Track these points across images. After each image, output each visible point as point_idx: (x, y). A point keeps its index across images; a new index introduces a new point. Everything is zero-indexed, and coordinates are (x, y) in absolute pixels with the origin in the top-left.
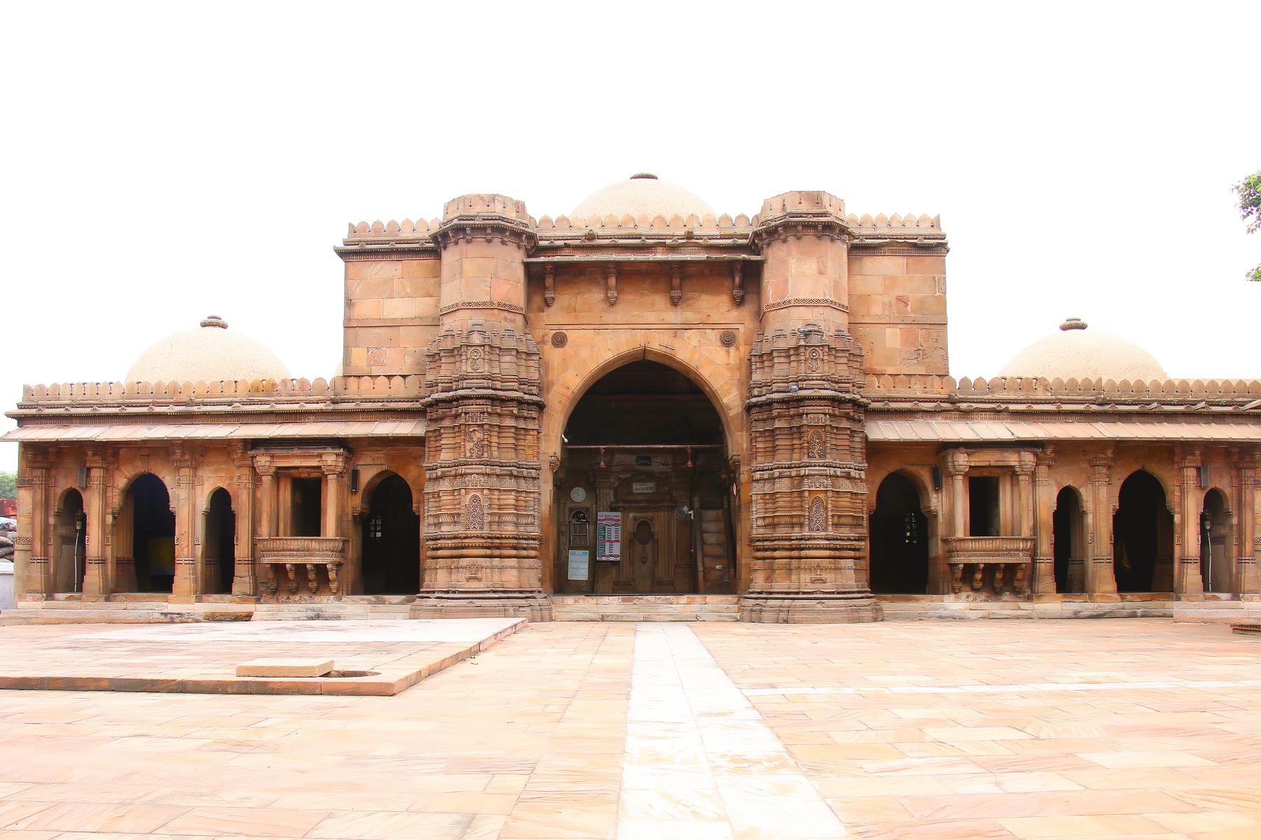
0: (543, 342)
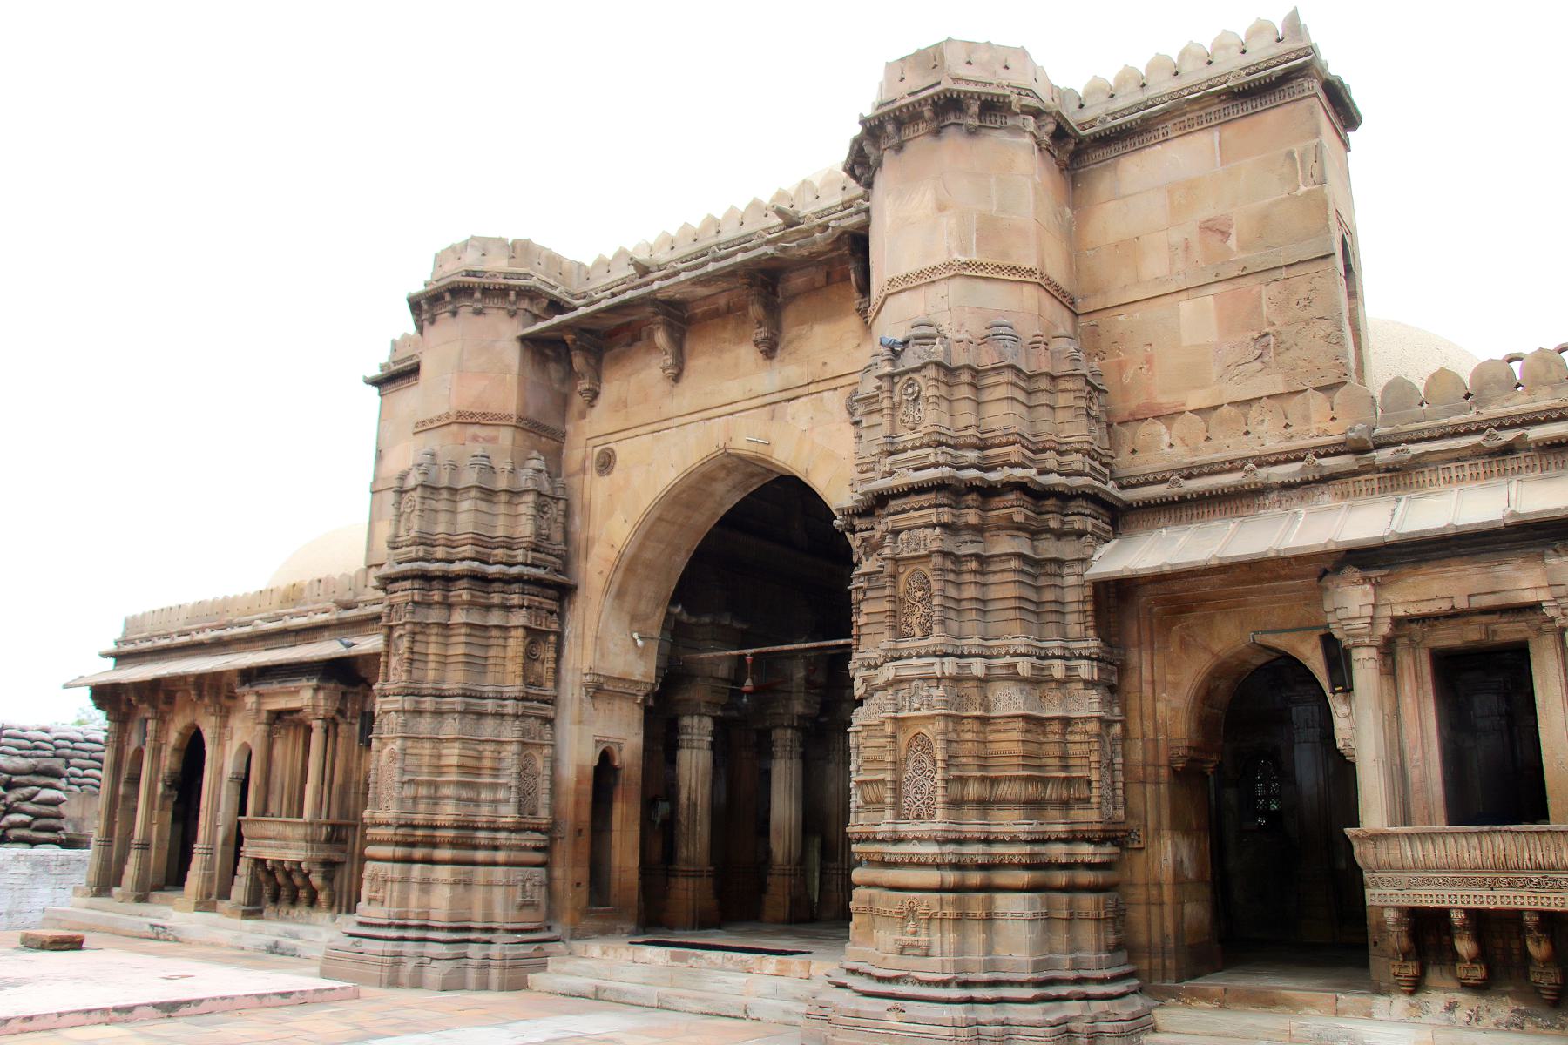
0: (583, 470)
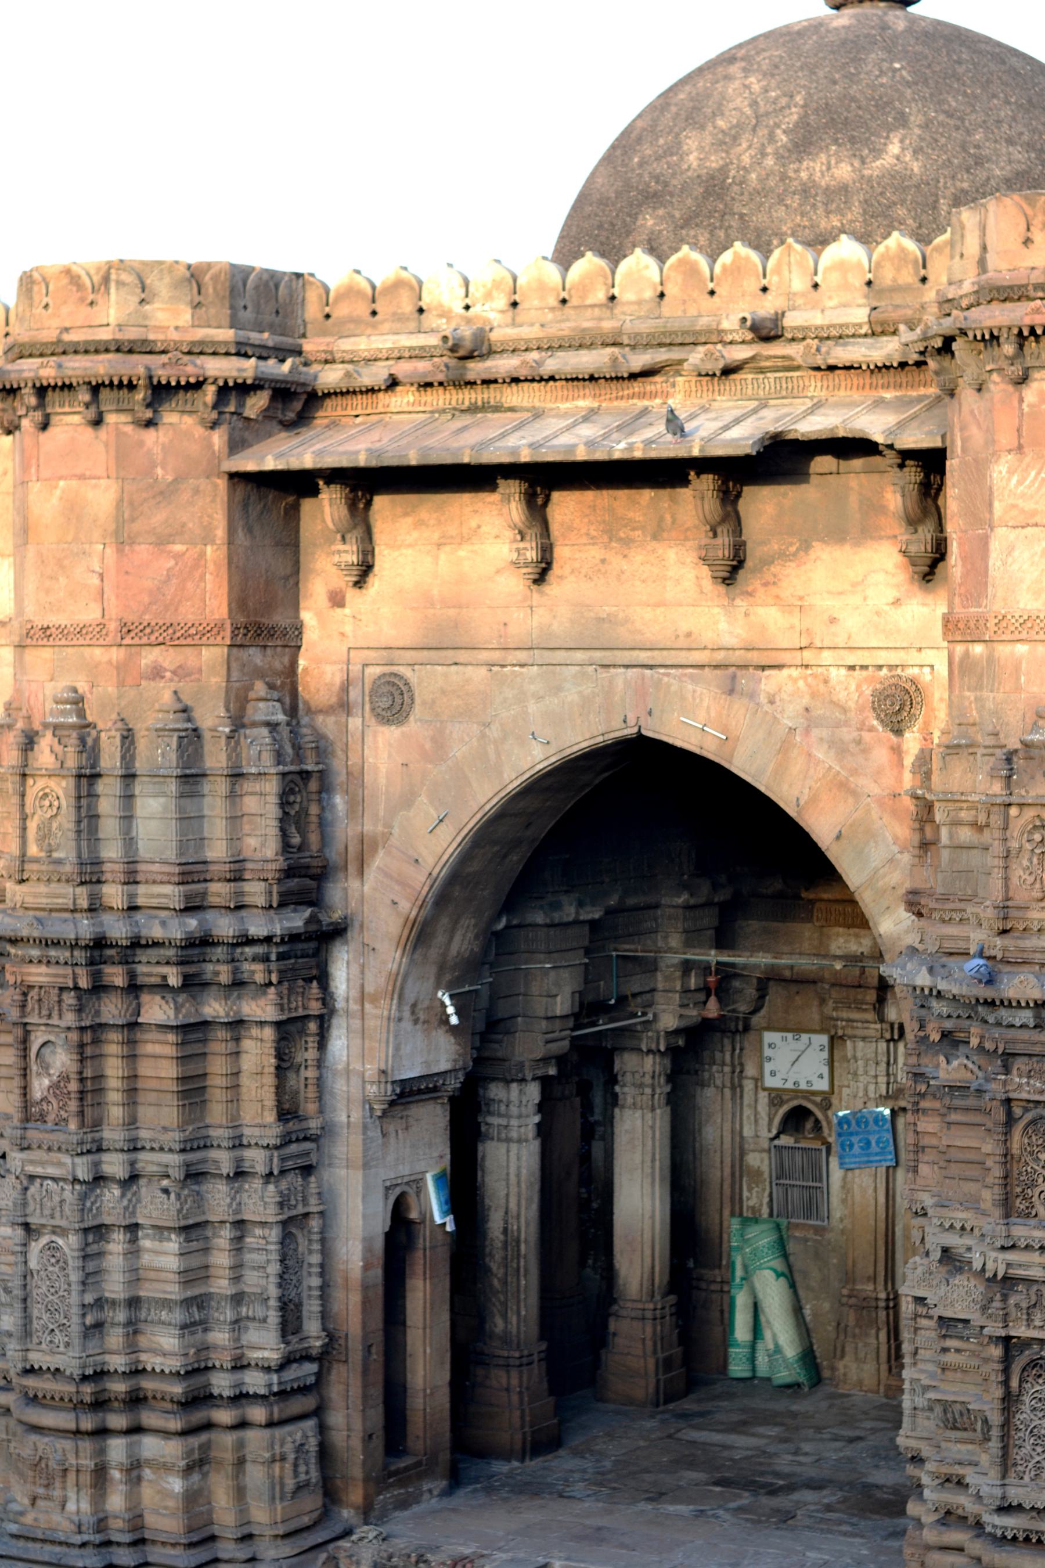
0: (344, 706)
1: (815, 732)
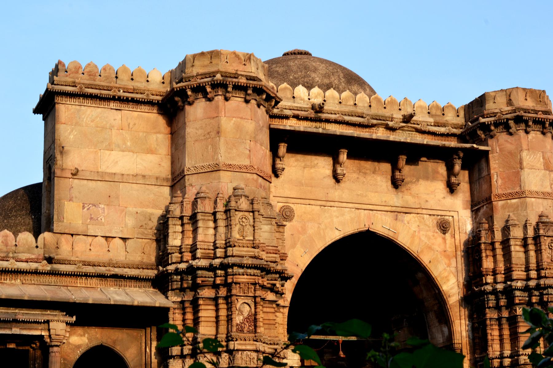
1: (421, 233)
